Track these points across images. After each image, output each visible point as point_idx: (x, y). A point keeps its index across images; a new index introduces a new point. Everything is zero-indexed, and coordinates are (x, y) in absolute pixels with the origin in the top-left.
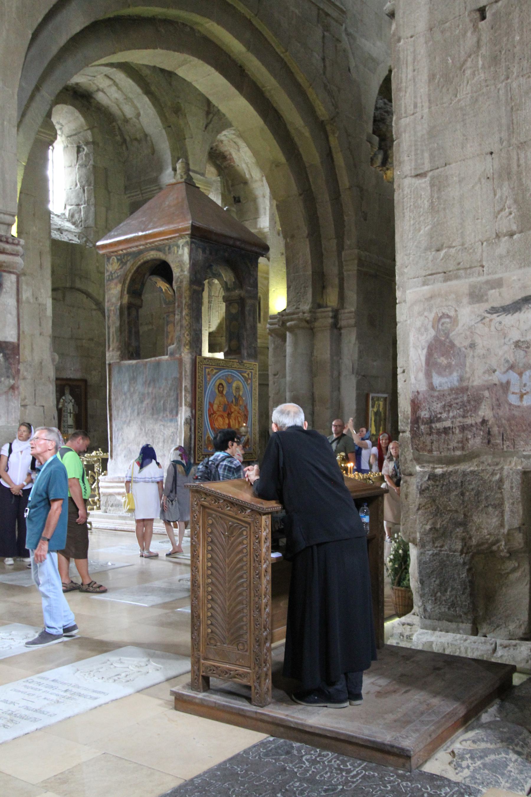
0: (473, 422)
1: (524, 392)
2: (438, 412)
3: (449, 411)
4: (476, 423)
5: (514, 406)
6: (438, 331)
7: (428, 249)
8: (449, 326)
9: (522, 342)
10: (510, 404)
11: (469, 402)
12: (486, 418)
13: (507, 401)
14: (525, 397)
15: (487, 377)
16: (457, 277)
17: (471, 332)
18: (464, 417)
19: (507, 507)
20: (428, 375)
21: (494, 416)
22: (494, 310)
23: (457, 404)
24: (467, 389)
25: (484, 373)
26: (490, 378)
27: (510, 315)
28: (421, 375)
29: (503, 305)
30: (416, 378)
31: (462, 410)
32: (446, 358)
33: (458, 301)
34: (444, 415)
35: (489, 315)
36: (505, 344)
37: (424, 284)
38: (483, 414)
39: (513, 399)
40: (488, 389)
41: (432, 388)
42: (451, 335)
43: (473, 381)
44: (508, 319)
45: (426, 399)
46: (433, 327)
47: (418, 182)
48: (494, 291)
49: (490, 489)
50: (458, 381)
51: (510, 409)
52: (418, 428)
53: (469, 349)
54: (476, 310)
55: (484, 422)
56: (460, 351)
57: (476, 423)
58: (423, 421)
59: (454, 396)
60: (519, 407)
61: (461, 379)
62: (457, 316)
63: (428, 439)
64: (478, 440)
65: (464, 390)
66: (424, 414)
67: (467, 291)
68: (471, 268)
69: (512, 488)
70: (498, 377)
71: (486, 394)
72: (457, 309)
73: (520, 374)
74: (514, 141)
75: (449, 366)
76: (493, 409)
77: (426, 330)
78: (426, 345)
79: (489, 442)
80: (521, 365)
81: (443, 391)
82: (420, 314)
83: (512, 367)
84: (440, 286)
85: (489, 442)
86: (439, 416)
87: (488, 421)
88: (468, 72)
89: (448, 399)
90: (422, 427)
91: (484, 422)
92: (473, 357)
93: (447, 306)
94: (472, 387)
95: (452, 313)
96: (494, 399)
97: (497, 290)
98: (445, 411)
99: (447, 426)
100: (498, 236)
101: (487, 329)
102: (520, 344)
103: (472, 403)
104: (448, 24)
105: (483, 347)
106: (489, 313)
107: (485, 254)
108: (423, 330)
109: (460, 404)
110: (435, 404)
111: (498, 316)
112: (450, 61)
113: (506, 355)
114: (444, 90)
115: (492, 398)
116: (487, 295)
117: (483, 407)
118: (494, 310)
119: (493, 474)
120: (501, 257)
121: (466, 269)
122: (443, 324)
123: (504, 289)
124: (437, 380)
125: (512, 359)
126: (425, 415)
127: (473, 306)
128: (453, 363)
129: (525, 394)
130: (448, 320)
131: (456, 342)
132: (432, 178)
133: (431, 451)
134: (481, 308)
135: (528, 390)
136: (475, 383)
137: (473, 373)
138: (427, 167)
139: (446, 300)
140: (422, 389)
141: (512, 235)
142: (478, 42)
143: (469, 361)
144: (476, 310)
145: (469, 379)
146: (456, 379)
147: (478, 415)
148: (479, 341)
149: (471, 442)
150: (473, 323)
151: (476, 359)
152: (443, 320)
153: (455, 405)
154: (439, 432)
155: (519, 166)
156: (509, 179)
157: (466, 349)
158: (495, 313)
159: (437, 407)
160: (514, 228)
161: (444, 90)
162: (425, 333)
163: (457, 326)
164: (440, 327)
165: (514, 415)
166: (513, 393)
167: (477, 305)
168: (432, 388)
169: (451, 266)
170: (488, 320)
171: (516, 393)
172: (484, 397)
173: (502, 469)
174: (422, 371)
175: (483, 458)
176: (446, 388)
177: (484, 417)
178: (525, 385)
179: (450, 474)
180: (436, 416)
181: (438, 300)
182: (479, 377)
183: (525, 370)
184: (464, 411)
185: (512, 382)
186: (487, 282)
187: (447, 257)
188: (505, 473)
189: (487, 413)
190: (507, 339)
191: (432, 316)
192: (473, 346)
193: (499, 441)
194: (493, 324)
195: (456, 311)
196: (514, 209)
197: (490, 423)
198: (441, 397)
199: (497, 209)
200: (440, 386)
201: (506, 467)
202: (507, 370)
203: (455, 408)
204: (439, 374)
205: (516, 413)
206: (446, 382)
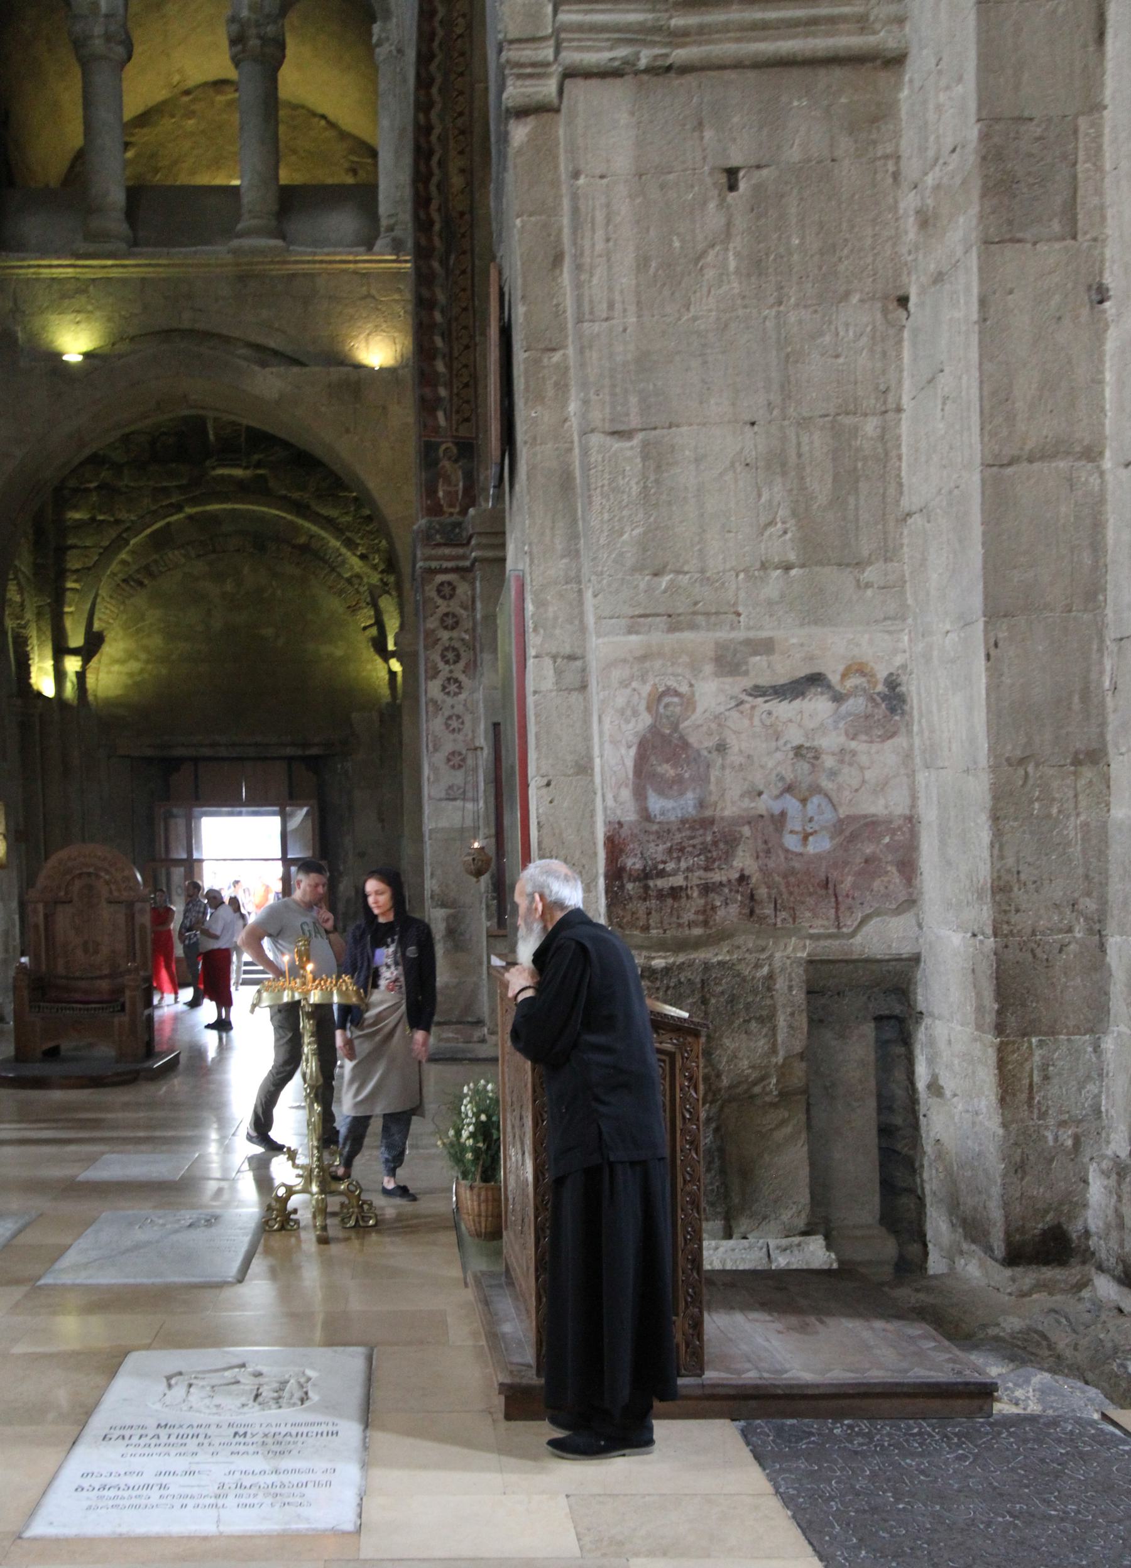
0: (724, 879)
1: (810, 831)
2: (659, 859)
3: (679, 859)
4: (729, 881)
5: (793, 853)
6: (657, 717)
7: (637, 569)
8: (678, 710)
9: (808, 748)
10: (787, 851)
11: (715, 843)
12: (747, 873)
13: (781, 846)
14: (811, 838)
15: (746, 803)
16: (693, 627)
17: (719, 725)
18: (707, 869)
19: (782, 1021)
20: (640, 794)
21: (761, 870)
22: (758, 691)
23: (694, 846)
24: (712, 821)
25: (742, 796)
26: (753, 805)
27: (786, 701)
28: (626, 794)
29: (774, 684)
30: (615, 798)
31: (702, 857)
32: (674, 766)
33: (694, 668)
34: (670, 866)
35: (750, 699)
36: (777, 749)
37: (631, 630)
38: (741, 865)
39: (791, 842)
40: (749, 823)
41: (646, 816)
42: (682, 726)
43: (722, 809)
44: (784, 709)
45: (636, 836)
46: (649, 709)
47: (617, 445)
48: (758, 658)
49: (755, 991)
50: (695, 806)
51: (786, 858)
52: (622, 887)
53: (715, 754)
54: (727, 687)
55: (743, 878)
56: (699, 755)
57: (729, 881)
58: (631, 875)
59: (688, 833)
60: (801, 854)
61: (701, 804)
62: (693, 694)
63: (641, 908)
64: (734, 909)
65: (707, 823)
66: (633, 863)
67: (711, 654)
68: (717, 613)
69: (790, 988)
70: (766, 804)
71: (746, 831)
72: (693, 682)
73: (804, 801)
74: (791, 411)
75: (679, 780)
76: (758, 857)
77: (635, 713)
78: (636, 740)
79: (752, 913)
80: (804, 786)
81: (668, 823)
82: (624, 684)
83: (789, 789)
84: (658, 637)
85: (752, 913)
86: (661, 866)
87: (749, 877)
88: (710, 274)
89: (678, 837)
90: (629, 886)
91: (743, 878)
92: (723, 767)
93: (673, 674)
94: (722, 818)
95: (684, 689)
96: (760, 841)
97: (764, 658)
98: (671, 859)
99: (675, 885)
100: (764, 566)
101: (746, 722)
102: (804, 752)
103: (722, 846)
104: (671, 177)
105: (741, 751)
106: (751, 695)
107: (742, 595)
108: (629, 712)
109: (699, 847)
110: (652, 845)
111: (766, 702)
112: (677, 244)
113: (779, 769)
114: (666, 292)
115: (756, 839)
116: (746, 663)
117: (741, 854)
118: (758, 691)
119: (757, 966)
120: (770, 603)
121: (707, 614)
122: (667, 706)
123: (775, 658)
124: (656, 804)
125: (789, 776)
126: (634, 864)
127: (721, 679)
128: (687, 775)
129: (811, 834)
130: (676, 700)
131: (692, 740)
132: (645, 444)
133: (646, 928)
134: (736, 685)
135: (817, 827)
136: (727, 813)
137: (723, 795)
138: (634, 421)
139: (673, 664)
140: (628, 819)
141: (788, 568)
142: (729, 224)
143: (714, 774)
144: (727, 687)
145: (715, 804)
146: (691, 803)
147: (731, 866)
148: (732, 741)
149: (721, 913)
150: (722, 709)
151: (728, 771)
152: (666, 700)
153: (690, 849)
154: (661, 895)
155: (799, 455)
156: (784, 474)
157: (710, 752)
158: (761, 696)
159: (657, 851)
160: (792, 557)
161: (666, 292)
162: (633, 720)
163: (694, 710)
164: (661, 710)
165: (793, 868)
166: (791, 832)
167: (729, 680)
168: (646, 816)
169: (681, 606)
170: (747, 706)
171: (796, 833)
172: (742, 836)
173: (771, 956)
174: (627, 786)
175: (739, 940)
176: (673, 818)
177: (742, 870)
178: (811, 820)
179: (681, 967)
180: (656, 868)
181: (658, 664)
182: (733, 803)
183: (811, 795)
184: (707, 859)
185: (791, 812)
186: (748, 642)
187: (672, 588)
188: (777, 964)
189: (747, 863)
190: (781, 742)
191: (646, 689)
192: (721, 748)
193: (768, 911)
194: (757, 713)
195: (691, 685)
196: (791, 523)
197: (754, 880)
198: (664, 833)
199: (763, 520)
200: (662, 814)
201: (778, 955)
202: (782, 794)
203: (691, 853)
204: (661, 793)
205: (797, 865)
206: (674, 808)
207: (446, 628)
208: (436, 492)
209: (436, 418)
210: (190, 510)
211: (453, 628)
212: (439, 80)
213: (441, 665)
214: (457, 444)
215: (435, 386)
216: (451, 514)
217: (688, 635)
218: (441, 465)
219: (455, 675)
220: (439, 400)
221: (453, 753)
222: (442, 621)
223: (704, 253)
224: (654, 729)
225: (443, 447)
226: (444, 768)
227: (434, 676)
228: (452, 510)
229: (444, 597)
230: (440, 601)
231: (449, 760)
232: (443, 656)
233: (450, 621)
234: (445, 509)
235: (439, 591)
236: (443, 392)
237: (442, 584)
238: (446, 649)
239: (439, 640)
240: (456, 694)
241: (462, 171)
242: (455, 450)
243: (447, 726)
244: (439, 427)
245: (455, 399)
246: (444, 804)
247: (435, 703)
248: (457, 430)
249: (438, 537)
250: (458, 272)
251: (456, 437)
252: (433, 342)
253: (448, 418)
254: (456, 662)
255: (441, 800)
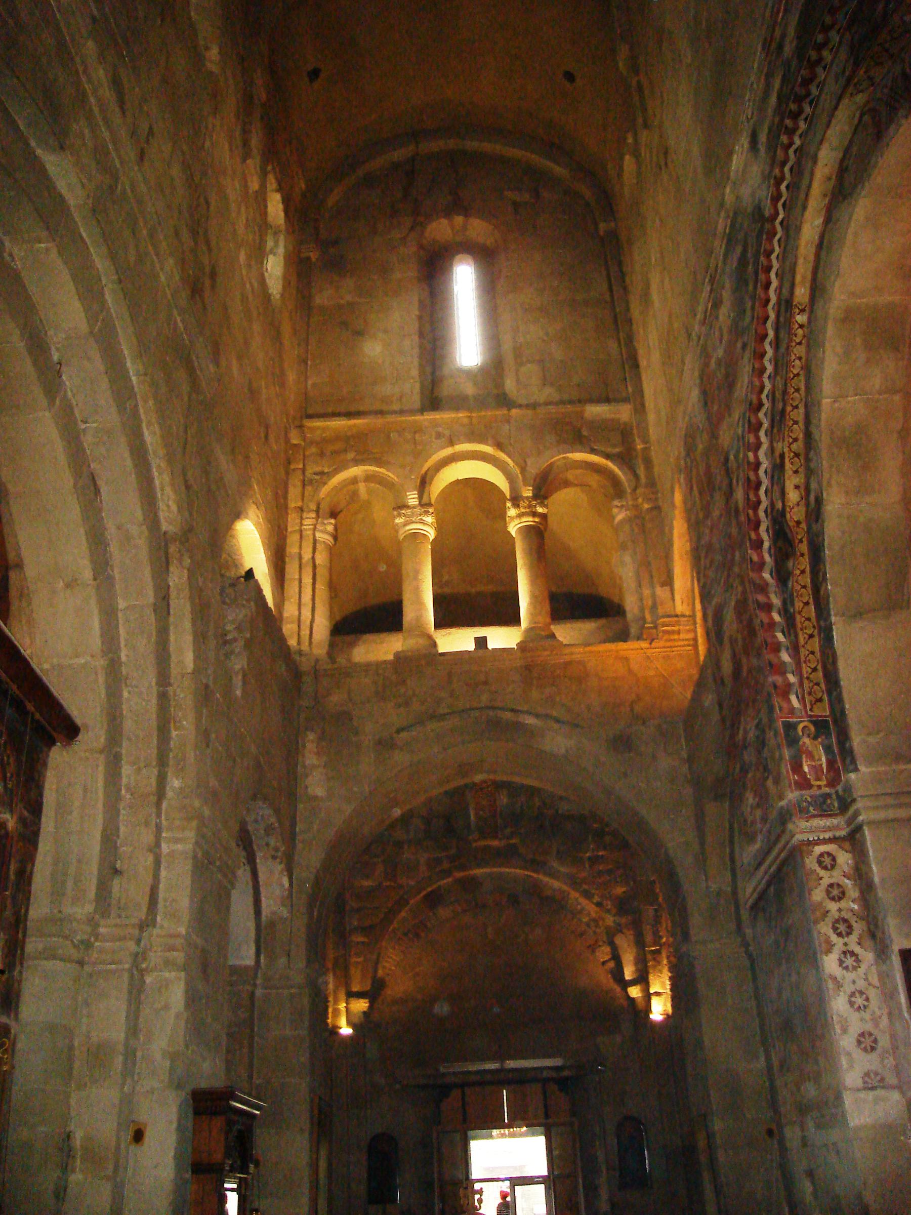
207: (833, 899)
208: (801, 766)
209: (789, 701)
211: (840, 899)
212: (766, 425)
213: (834, 938)
214: (811, 722)
215: (783, 674)
216: (819, 787)
218: (801, 743)
219: (850, 948)
220: (789, 685)
221: (862, 1035)
222: (828, 892)
225: (801, 726)
226: (858, 1054)
227: (829, 951)
228: (818, 783)
229: (825, 868)
230: (822, 873)
231: (859, 1042)
232: (835, 929)
233: (835, 892)
234: (813, 782)
235: (819, 862)
236: (792, 679)
237: (822, 855)
238: (837, 921)
239: (827, 912)
240: (855, 968)
241: (797, 487)
242: (812, 728)
243: (852, 1004)
244: (794, 708)
245: (806, 682)
246: (862, 1095)
247: (834, 979)
248: (810, 710)
249: (811, 809)
250: (798, 572)
251: (811, 716)
252: (775, 637)
253: (802, 700)
254: (849, 934)
255: (858, 1090)
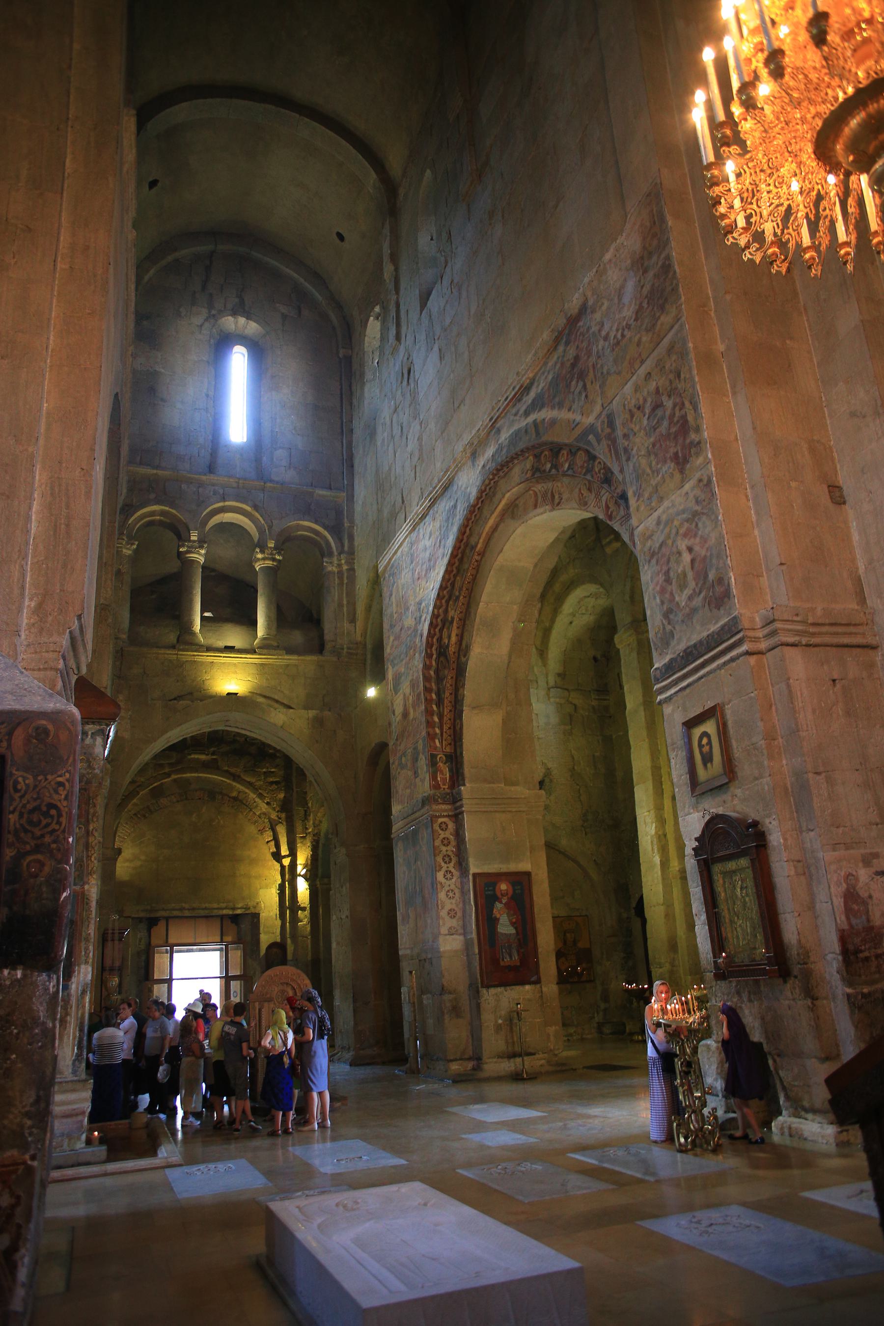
3: (865, 945)
6: (848, 884)
16: (853, 848)
18: (875, 948)
20: (848, 918)
28: (843, 918)
34: (863, 947)
68: (859, 842)
95: (854, 873)
121: (856, 843)
124: (854, 921)
130: (853, 878)
131: (861, 894)
136: (877, 924)
150: (867, 881)
192: (870, 897)
210: (174, 777)
217: (852, 851)
223: (831, 708)
224: (848, 889)
